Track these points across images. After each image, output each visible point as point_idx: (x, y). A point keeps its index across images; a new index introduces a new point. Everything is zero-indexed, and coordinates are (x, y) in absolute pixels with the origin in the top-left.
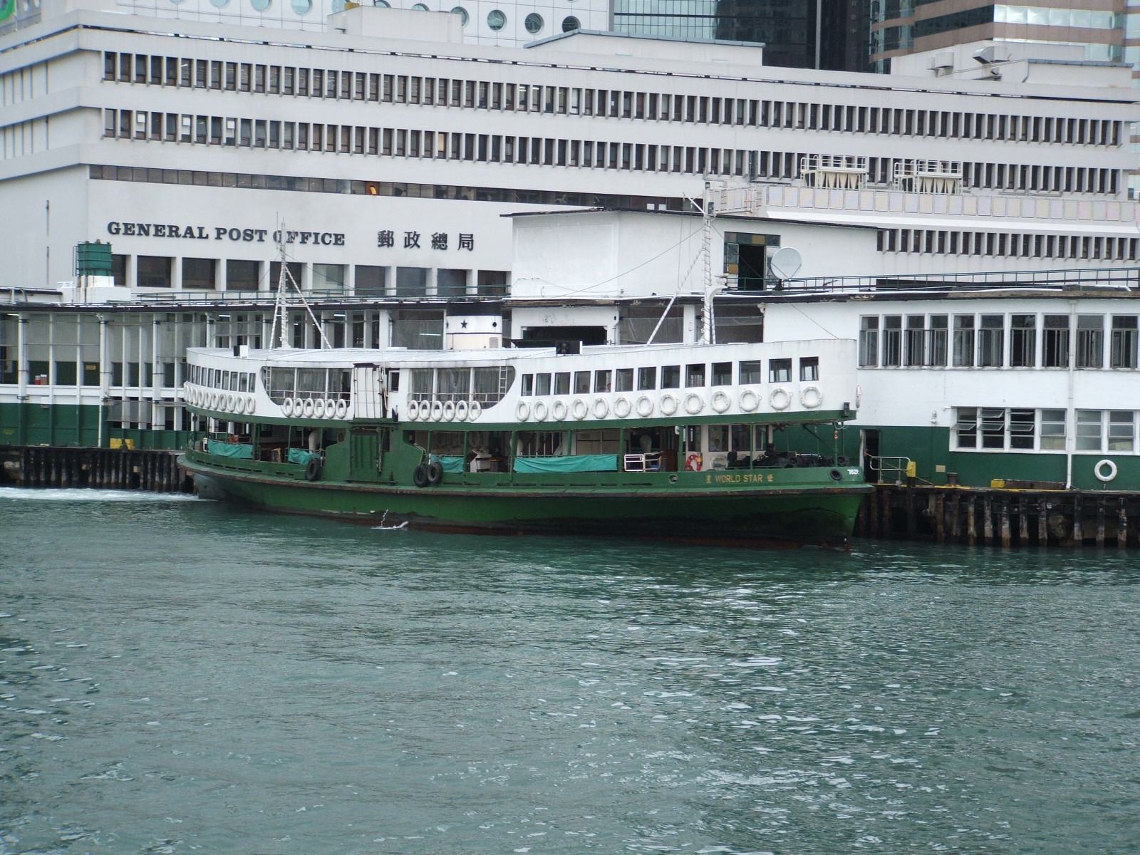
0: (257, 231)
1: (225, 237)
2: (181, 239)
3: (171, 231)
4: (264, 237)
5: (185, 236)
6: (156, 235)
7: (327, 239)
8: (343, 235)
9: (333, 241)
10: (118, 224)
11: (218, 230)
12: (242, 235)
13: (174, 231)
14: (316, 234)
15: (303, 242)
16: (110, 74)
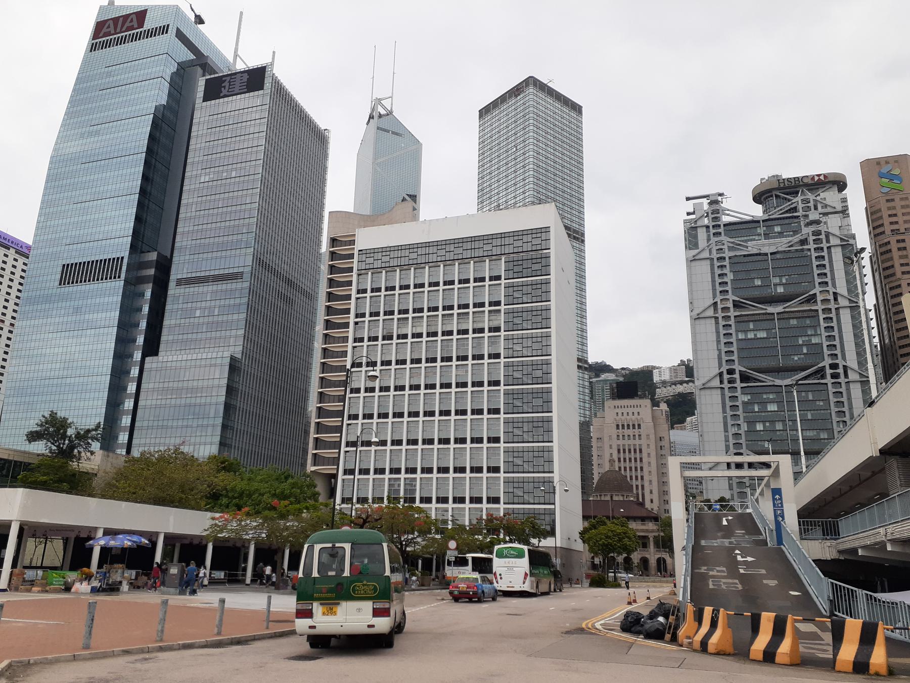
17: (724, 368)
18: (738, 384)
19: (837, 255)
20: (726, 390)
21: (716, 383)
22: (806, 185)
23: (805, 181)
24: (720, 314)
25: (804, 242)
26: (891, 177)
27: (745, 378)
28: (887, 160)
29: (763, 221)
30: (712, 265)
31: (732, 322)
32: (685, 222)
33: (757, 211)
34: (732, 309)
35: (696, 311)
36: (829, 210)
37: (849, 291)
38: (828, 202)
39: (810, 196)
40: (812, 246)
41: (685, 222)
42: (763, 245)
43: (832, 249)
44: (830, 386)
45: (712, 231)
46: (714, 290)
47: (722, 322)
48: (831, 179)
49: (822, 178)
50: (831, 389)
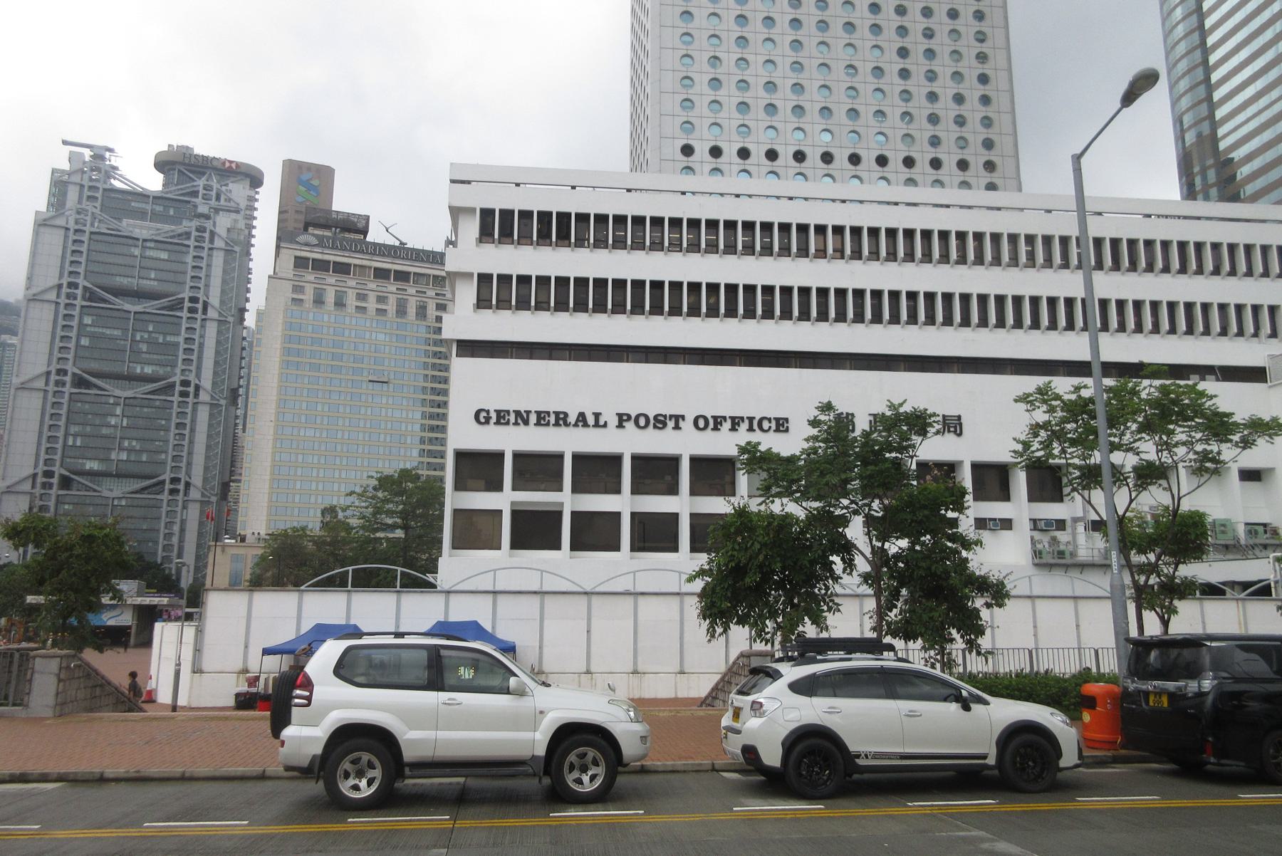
0: (671, 416)
1: (630, 425)
2: (571, 428)
3: (557, 419)
4: (681, 424)
5: (576, 425)
6: (538, 424)
7: (766, 425)
8: (787, 420)
9: (774, 427)
10: (488, 412)
11: (620, 416)
12: (652, 421)
13: (561, 419)
14: (751, 419)
15: (733, 429)
16: (485, 234)
17: (53, 369)
18: (68, 389)
19: (218, 260)
20: (50, 395)
21: (40, 384)
22: (215, 169)
23: (215, 163)
24: (63, 300)
25: (188, 235)
26: (309, 187)
27: (80, 382)
28: (310, 167)
29: (154, 198)
30: (66, 237)
31: (76, 312)
32: (54, 171)
33: (153, 182)
34: (79, 297)
35: (34, 290)
36: (232, 204)
37: (222, 302)
38: (234, 196)
39: (214, 183)
40: (192, 243)
41: (54, 171)
42: (142, 227)
43: (215, 253)
44: (175, 404)
45: (86, 193)
46: (62, 267)
47: (62, 311)
48: (243, 170)
49: (234, 166)
50: (175, 409)
